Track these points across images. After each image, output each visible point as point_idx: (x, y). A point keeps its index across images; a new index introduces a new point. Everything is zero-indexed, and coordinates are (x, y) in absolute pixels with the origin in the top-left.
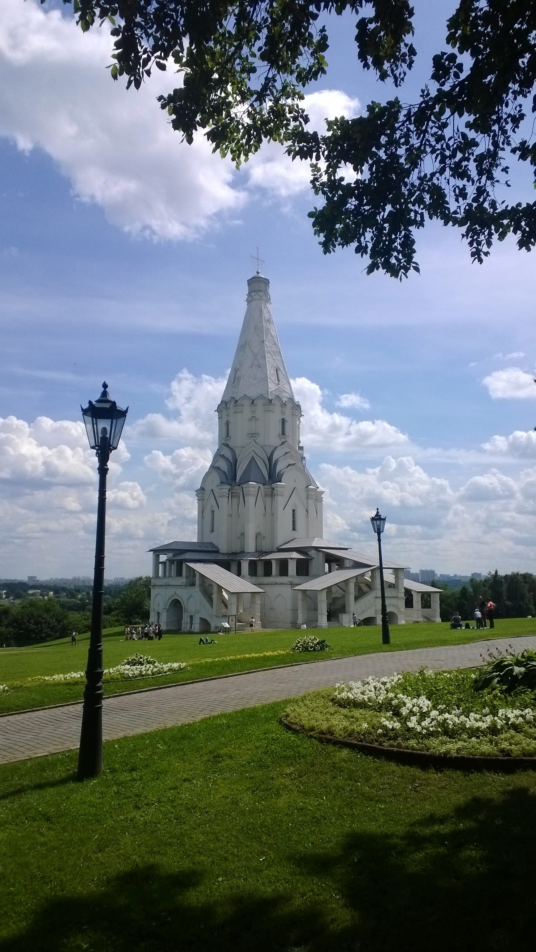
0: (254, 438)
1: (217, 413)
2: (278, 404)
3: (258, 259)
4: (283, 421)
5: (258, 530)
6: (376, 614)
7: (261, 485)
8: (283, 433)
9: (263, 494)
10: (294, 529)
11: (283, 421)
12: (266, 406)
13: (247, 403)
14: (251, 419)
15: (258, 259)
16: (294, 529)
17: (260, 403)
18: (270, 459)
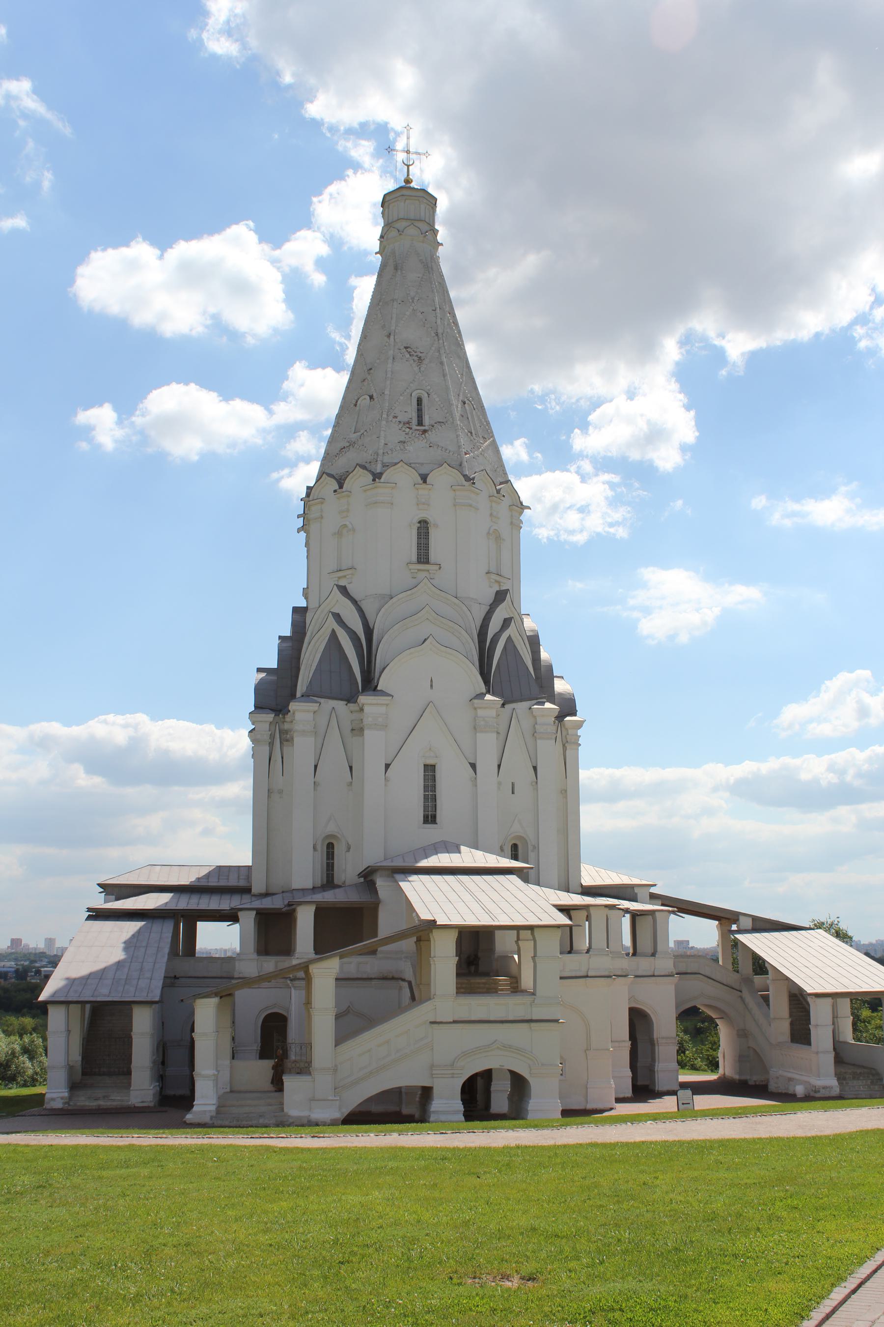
1: (303, 534)
3: (408, 152)
4: (424, 529)
5: (331, 829)
8: (423, 557)
10: (430, 818)
11: (424, 529)
14: (339, 534)
15: (408, 152)
16: (430, 818)
18: (369, 632)
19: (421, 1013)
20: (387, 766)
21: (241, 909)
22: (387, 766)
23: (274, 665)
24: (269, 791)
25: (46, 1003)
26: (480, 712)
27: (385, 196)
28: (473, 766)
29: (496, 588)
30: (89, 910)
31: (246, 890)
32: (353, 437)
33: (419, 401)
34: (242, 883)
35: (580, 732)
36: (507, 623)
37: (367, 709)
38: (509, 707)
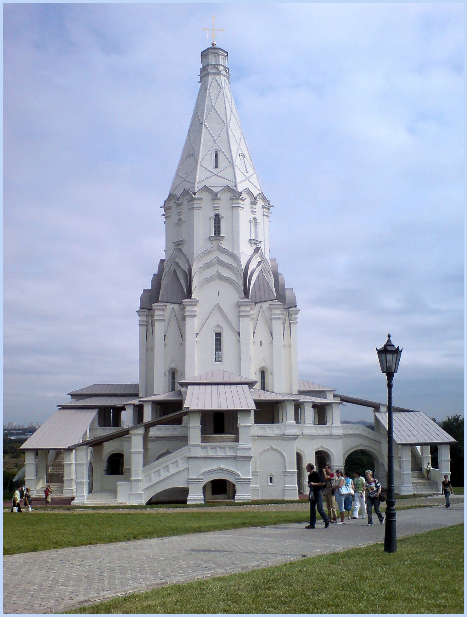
0: (180, 247)
2: (207, 197)
4: (217, 219)
5: (173, 365)
6: (188, 483)
7: (176, 307)
9: (180, 317)
10: (218, 359)
11: (217, 219)
12: (191, 203)
13: (172, 204)
16: (218, 359)
17: (185, 201)
19: (183, 452)
20: (197, 335)
21: (126, 405)
22: (197, 335)
23: (149, 288)
24: (147, 349)
25: (24, 451)
26: (242, 308)
27: (202, 53)
28: (239, 333)
29: (255, 247)
30: (59, 406)
31: (136, 395)
32: (184, 176)
33: (216, 155)
34: (135, 392)
35: (297, 316)
36: (260, 263)
37: (187, 308)
38: (258, 305)
